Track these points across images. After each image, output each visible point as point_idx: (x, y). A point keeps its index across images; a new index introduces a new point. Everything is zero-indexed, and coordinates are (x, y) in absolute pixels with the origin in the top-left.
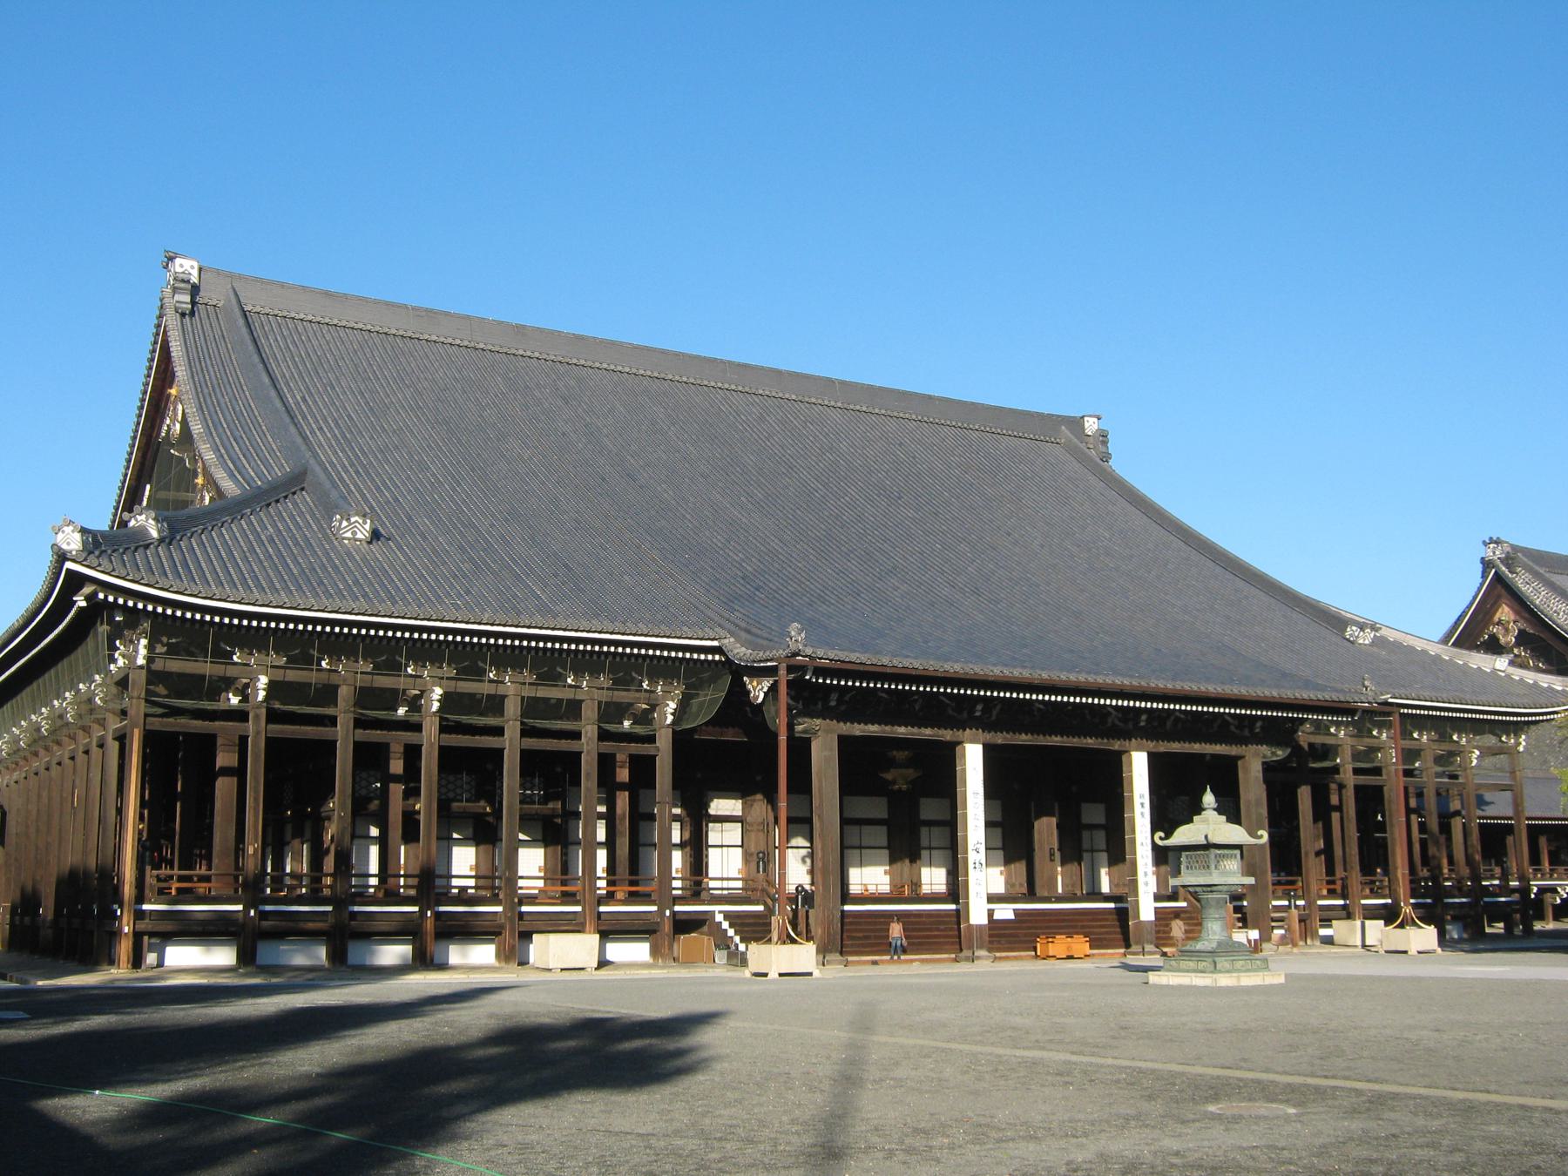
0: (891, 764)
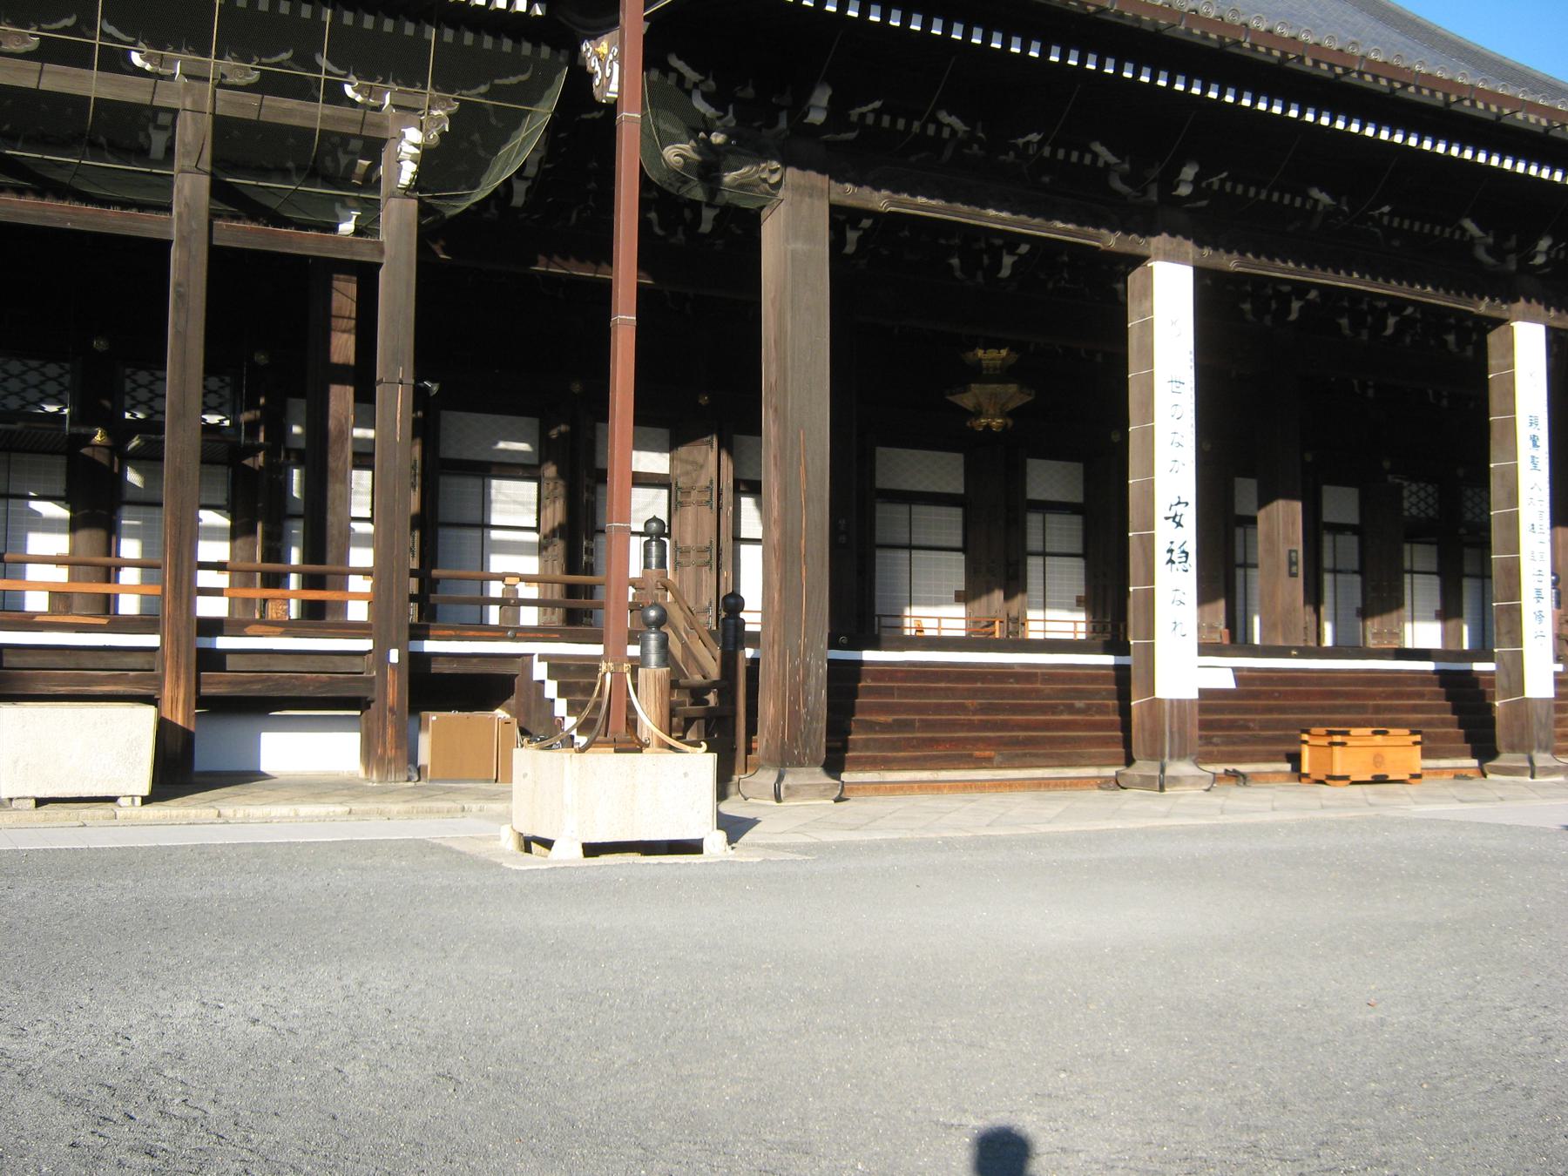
0: (977, 374)
